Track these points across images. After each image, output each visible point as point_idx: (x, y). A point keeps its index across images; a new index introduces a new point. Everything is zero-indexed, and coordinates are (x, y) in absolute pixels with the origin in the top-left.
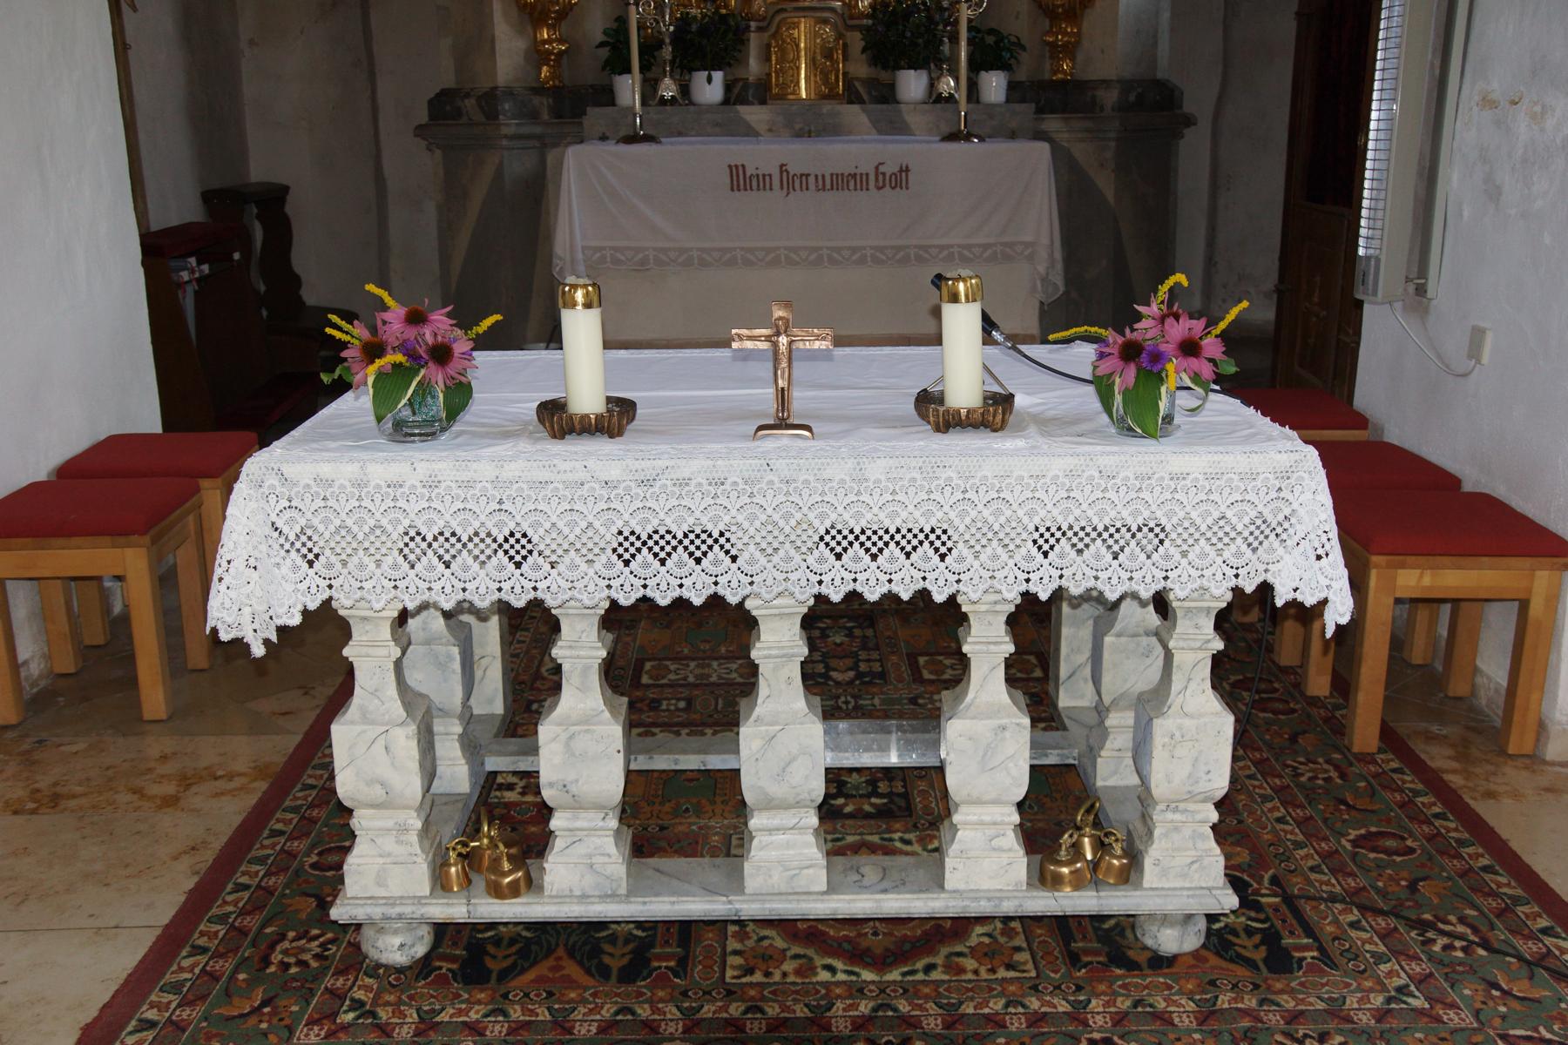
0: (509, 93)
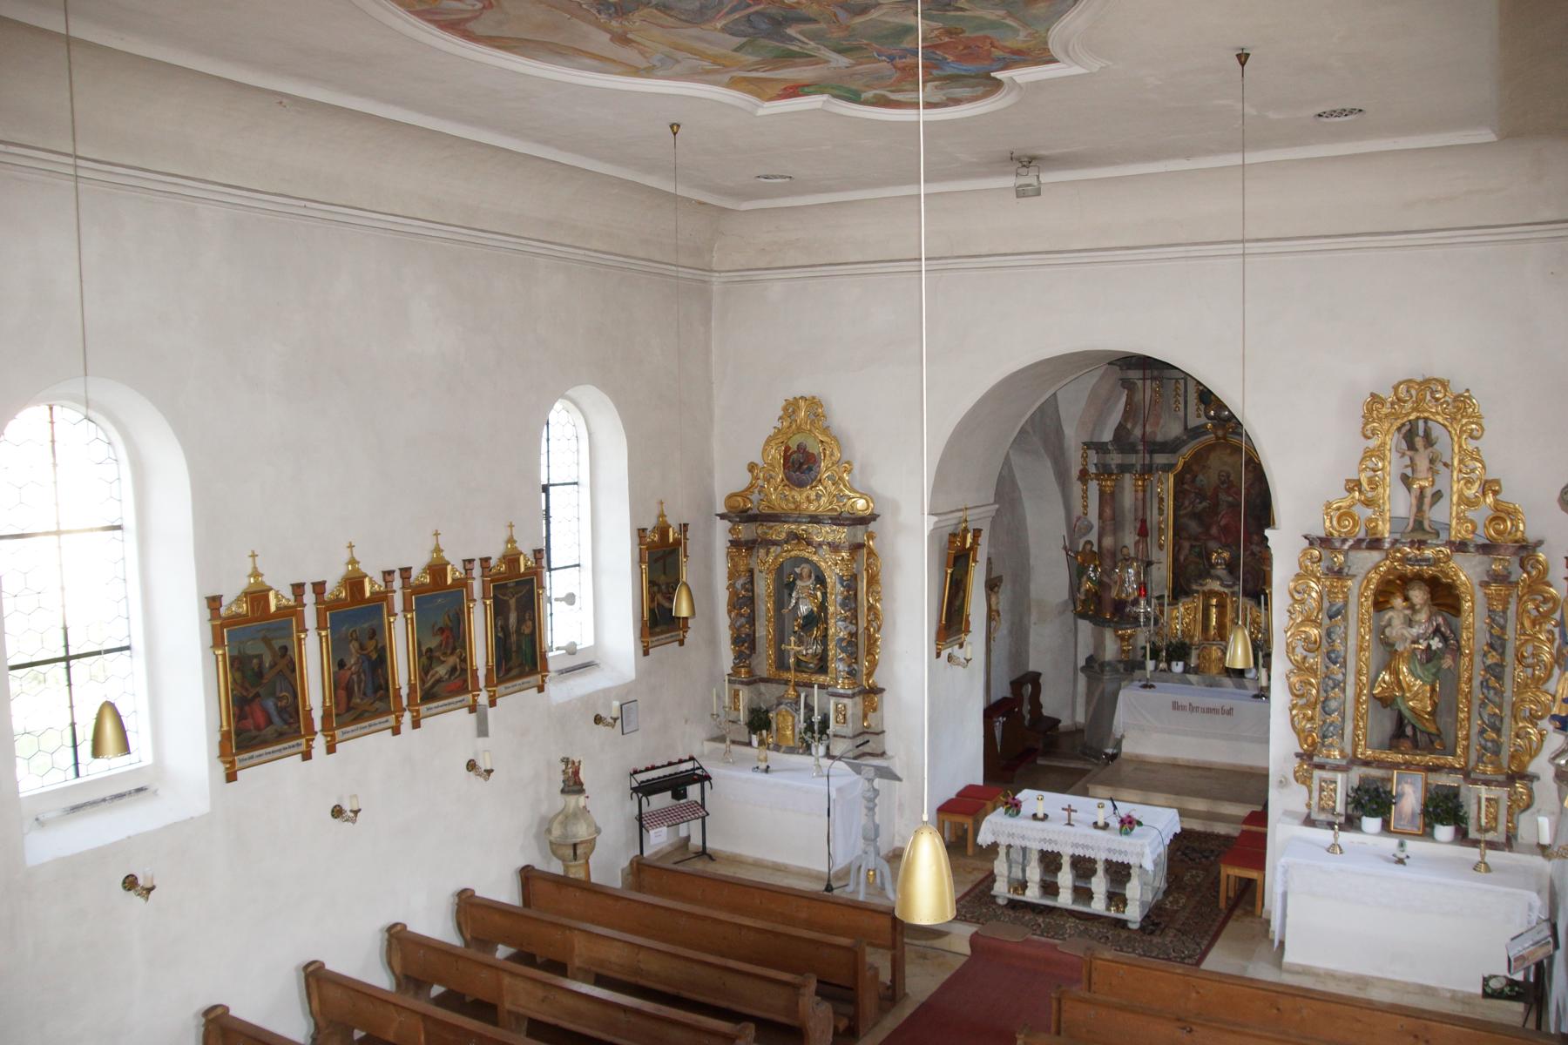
0: (1109, 664)
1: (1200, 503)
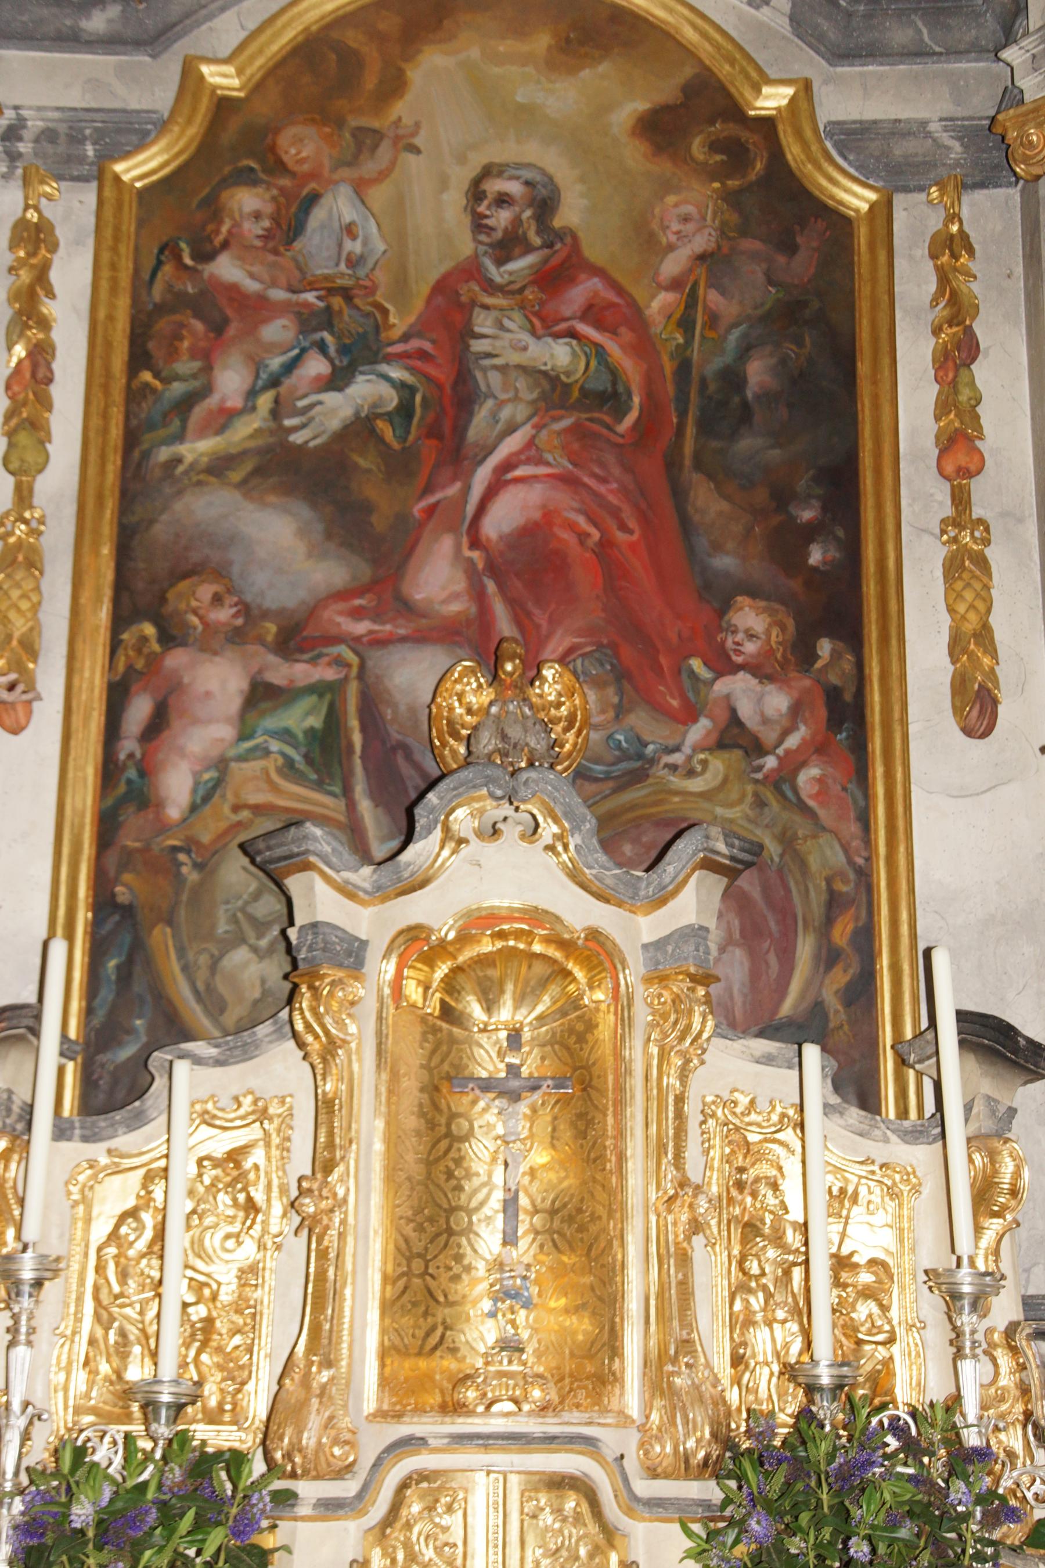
1: (337, 380)
